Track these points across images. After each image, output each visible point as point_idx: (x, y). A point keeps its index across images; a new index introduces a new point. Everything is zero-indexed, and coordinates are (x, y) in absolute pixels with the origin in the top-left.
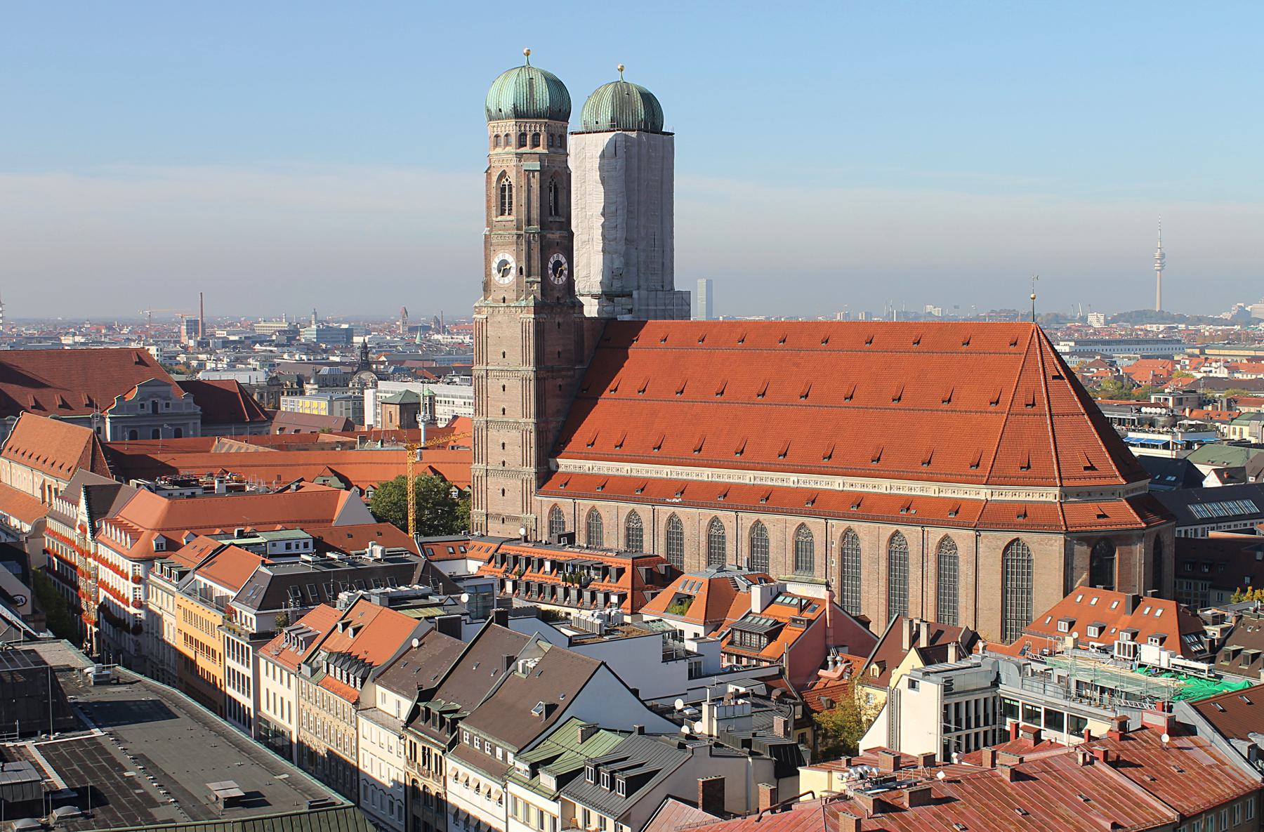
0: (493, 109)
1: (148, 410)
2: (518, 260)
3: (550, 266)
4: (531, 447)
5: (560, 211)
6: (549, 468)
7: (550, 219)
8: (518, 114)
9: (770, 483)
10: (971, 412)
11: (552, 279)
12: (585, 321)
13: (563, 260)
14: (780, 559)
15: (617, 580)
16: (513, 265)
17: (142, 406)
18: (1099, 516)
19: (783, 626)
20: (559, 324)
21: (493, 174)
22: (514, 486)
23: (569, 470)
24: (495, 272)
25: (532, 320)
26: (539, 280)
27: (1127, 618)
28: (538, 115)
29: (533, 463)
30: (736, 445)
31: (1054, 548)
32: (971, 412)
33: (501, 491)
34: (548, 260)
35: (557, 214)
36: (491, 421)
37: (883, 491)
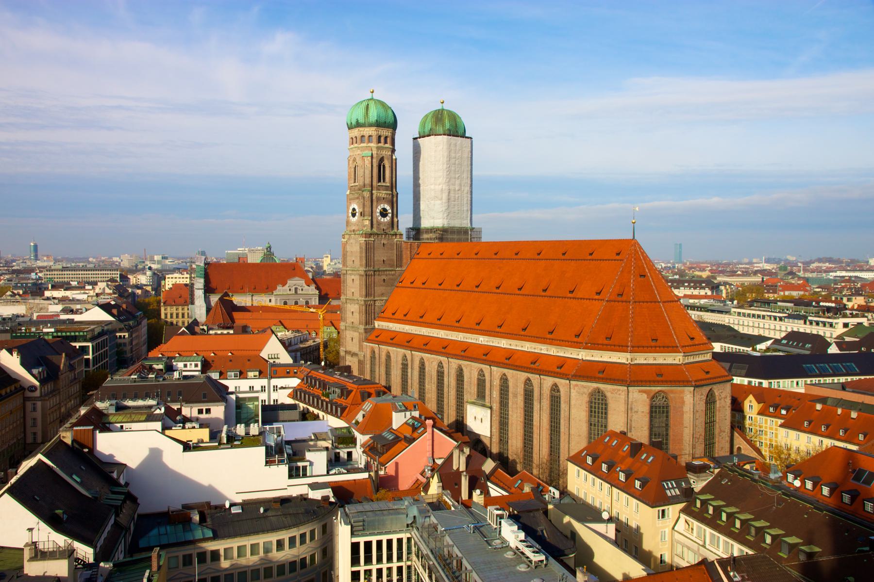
2: (359, 208)
7: (379, 184)
9: (470, 341)
10: (584, 299)
11: (379, 218)
15: (347, 398)
17: (290, 290)
18: (658, 375)
19: (400, 441)
22: (356, 335)
23: (384, 328)
26: (370, 218)
27: (630, 460)
28: (371, 125)
30: (457, 317)
31: (621, 396)
32: (584, 299)
34: (377, 208)
35: (384, 181)
37: (526, 350)
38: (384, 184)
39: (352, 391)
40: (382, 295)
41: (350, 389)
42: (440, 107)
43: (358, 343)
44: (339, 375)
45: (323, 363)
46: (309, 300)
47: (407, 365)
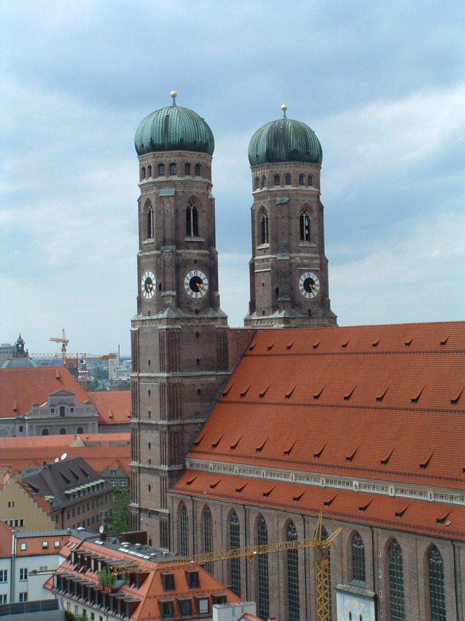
0: (139, 145)
1: (57, 413)
3: (187, 281)
4: (166, 447)
5: (200, 232)
6: (185, 466)
7: (187, 239)
8: (154, 147)
9: (338, 486)
12: (228, 331)
13: (202, 275)
14: (338, 566)
16: (154, 282)
17: (52, 411)
20: (197, 334)
21: (142, 202)
22: (155, 481)
24: (143, 288)
25: (165, 331)
26: (174, 293)
28: (173, 147)
29: (167, 462)
33: (148, 487)
34: (185, 276)
35: (196, 234)
36: (142, 424)
38: (196, 239)
39: (148, 574)
40: (197, 414)
41: (144, 570)
42: (280, 117)
43: (159, 494)
44: (127, 548)
45: (101, 530)
46: (83, 427)
47: (237, 528)
